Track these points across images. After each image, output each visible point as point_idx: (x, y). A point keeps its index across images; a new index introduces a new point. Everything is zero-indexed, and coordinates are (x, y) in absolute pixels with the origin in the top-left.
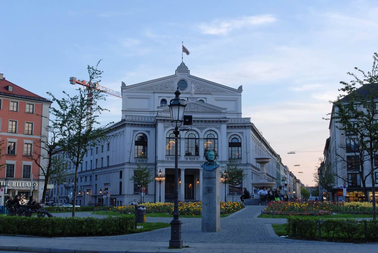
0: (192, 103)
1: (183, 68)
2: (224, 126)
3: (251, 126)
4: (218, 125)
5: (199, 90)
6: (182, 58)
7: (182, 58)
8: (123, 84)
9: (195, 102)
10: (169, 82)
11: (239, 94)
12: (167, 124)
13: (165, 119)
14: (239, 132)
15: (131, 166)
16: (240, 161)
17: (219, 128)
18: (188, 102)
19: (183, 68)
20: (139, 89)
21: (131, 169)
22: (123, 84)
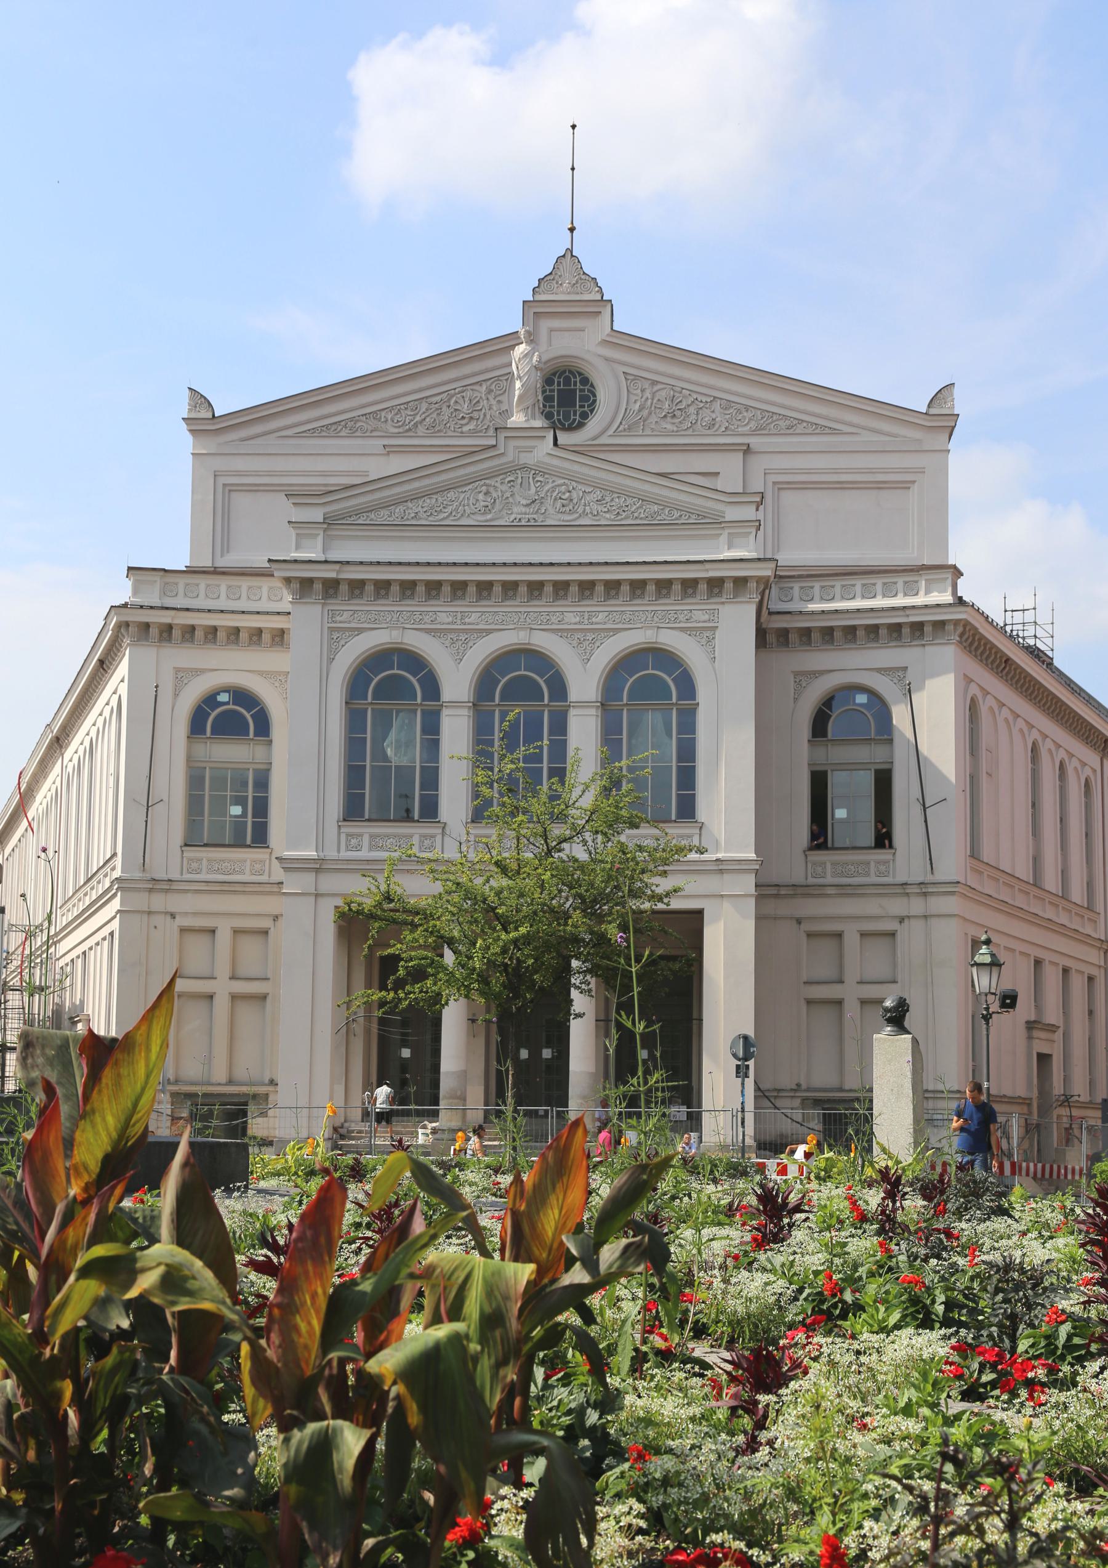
0: (524, 468)
1: (567, 294)
2: (737, 621)
3: (956, 622)
4: (697, 610)
5: (669, 427)
6: (572, 230)
7: (572, 230)
8: (198, 399)
9: (547, 460)
10: (479, 383)
11: (936, 441)
12: (347, 611)
13: (333, 575)
14: (879, 670)
15: (158, 902)
16: (886, 862)
17: (706, 633)
18: (496, 462)
19: (567, 294)
20: (298, 436)
21: (158, 920)
22: (198, 399)
